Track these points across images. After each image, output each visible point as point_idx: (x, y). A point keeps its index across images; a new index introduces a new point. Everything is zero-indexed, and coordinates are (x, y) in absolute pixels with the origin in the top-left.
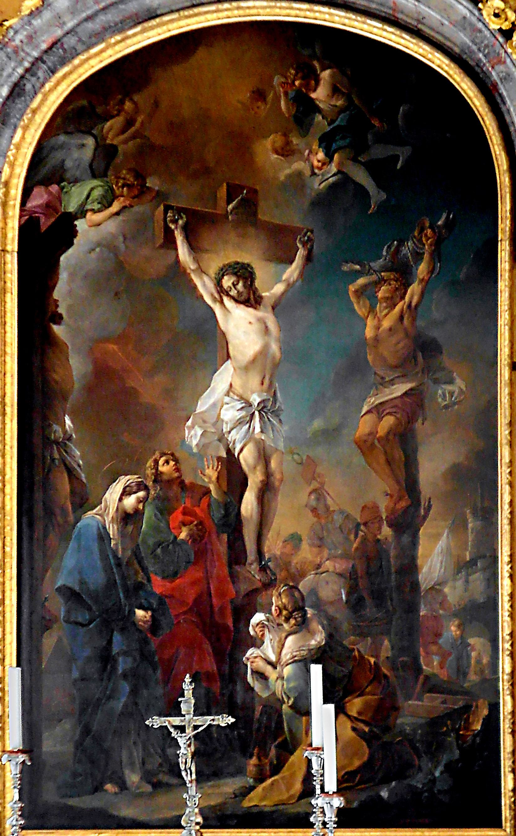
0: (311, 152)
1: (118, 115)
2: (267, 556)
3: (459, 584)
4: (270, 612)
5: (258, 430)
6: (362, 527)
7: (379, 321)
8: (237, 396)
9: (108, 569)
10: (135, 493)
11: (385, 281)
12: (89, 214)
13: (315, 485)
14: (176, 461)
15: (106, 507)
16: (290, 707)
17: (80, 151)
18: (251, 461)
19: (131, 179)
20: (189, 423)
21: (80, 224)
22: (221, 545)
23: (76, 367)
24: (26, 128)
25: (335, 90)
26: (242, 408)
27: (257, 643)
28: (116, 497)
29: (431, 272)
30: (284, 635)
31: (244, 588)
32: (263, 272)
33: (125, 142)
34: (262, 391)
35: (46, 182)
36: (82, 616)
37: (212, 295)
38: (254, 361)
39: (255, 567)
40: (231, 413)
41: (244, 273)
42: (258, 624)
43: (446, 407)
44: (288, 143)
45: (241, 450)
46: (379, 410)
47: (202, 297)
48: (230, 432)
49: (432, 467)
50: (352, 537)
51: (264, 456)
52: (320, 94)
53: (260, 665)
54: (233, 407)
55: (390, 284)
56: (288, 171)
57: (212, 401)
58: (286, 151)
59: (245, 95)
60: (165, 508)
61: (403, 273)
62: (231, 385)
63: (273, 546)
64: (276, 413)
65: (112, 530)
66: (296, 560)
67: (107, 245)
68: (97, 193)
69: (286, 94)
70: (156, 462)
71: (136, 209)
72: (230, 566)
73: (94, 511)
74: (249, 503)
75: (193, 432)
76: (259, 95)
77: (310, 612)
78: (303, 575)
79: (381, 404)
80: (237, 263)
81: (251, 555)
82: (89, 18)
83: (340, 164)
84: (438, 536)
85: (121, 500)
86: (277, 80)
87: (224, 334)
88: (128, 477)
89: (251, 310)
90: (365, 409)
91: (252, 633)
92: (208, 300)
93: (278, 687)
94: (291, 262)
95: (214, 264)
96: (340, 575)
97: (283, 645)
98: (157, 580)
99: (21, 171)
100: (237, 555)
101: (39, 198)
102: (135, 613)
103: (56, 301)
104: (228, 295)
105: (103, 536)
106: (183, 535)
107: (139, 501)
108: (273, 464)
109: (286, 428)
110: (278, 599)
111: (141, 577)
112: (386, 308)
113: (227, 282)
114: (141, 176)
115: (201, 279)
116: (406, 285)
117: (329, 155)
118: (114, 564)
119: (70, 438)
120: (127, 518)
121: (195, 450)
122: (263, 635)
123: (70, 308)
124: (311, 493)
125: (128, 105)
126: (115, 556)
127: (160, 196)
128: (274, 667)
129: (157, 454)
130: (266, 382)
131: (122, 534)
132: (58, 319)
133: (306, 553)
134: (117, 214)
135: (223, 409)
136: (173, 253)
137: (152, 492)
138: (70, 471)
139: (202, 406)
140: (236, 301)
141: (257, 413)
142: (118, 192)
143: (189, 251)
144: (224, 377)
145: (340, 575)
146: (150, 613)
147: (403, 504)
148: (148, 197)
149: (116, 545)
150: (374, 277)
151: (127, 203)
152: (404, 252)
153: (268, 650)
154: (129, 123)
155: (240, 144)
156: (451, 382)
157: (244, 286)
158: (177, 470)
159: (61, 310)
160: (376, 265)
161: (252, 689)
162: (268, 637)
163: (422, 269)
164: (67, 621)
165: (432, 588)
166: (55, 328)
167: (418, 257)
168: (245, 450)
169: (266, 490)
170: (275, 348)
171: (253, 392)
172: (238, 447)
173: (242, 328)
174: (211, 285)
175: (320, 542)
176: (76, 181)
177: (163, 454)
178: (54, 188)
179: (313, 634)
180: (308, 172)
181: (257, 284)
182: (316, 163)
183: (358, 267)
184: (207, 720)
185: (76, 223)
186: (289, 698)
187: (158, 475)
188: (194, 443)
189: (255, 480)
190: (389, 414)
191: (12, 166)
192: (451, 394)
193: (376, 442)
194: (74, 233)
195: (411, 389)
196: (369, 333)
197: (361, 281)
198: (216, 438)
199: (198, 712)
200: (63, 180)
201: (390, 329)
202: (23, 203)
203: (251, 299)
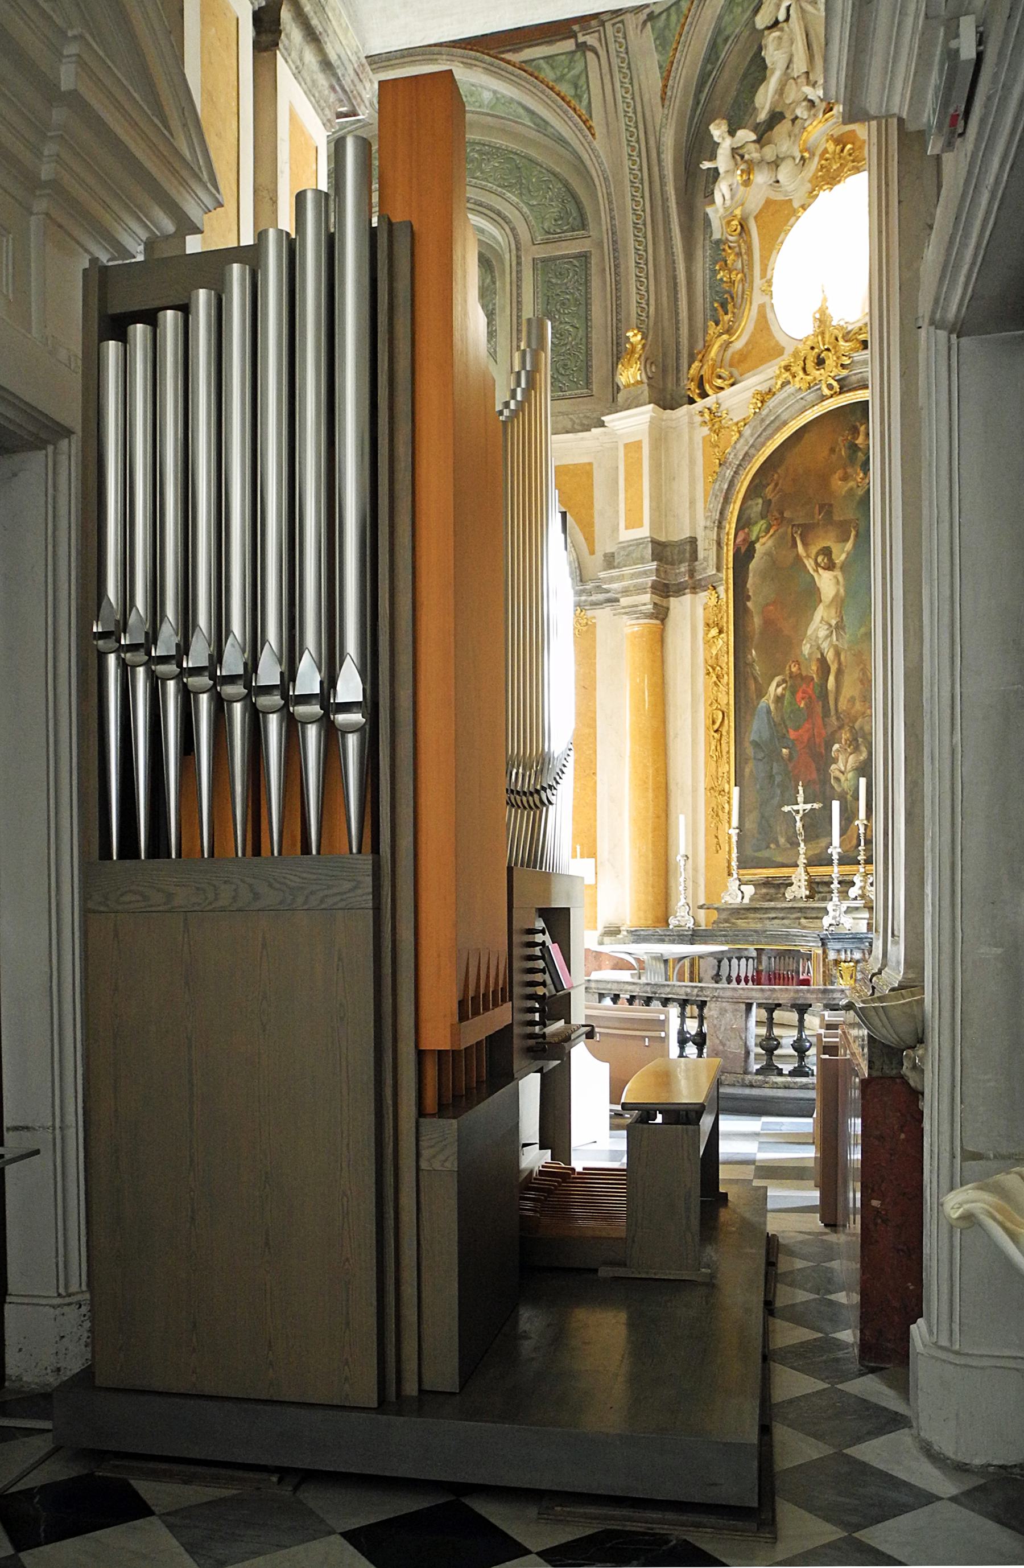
13: (862, 666)
18: (832, 658)
19: (778, 515)
21: (757, 546)
22: (819, 709)
23: (757, 621)
24: (735, 502)
27: (835, 761)
28: (774, 689)
31: (830, 730)
32: (835, 549)
35: (743, 528)
36: (761, 755)
38: (832, 601)
40: (822, 633)
41: (827, 552)
44: (846, 473)
51: (838, 654)
53: (837, 774)
58: (845, 478)
59: (826, 453)
63: (843, 705)
64: (843, 628)
65: (772, 707)
66: (853, 711)
67: (768, 554)
72: (823, 718)
76: (832, 450)
77: (860, 740)
78: (857, 720)
81: (833, 712)
82: (759, 436)
86: (840, 438)
87: (818, 589)
92: (811, 572)
93: (845, 785)
94: (847, 540)
95: (814, 550)
98: (791, 731)
99: (734, 525)
100: (826, 713)
105: (769, 711)
106: (802, 706)
107: (784, 689)
108: (842, 657)
110: (845, 735)
113: (820, 559)
114: (782, 513)
118: (773, 725)
120: (779, 699)
123: (754, 591)
125: (776, 476)
127: (790, 520)
128: (843, 773)
132: (748, 598)
138: (755, 678)
139: (809, 632)
140: (823, 568)
144: (820, 612)
148: (785, 522)
153: (841, 765)
154: (776, 485)
155: (824, 480)
158: (799, 669)
161: (833, 787)
170: (842, 591)
174: (813, 563)
176: (756, 523)
178: (746, 530)
181: (834, 557)
184: (808, 806)
187: (791, 672)
189: (834, 668)
191: (730, 523)
199: (805, 803)
203: (830, 567)
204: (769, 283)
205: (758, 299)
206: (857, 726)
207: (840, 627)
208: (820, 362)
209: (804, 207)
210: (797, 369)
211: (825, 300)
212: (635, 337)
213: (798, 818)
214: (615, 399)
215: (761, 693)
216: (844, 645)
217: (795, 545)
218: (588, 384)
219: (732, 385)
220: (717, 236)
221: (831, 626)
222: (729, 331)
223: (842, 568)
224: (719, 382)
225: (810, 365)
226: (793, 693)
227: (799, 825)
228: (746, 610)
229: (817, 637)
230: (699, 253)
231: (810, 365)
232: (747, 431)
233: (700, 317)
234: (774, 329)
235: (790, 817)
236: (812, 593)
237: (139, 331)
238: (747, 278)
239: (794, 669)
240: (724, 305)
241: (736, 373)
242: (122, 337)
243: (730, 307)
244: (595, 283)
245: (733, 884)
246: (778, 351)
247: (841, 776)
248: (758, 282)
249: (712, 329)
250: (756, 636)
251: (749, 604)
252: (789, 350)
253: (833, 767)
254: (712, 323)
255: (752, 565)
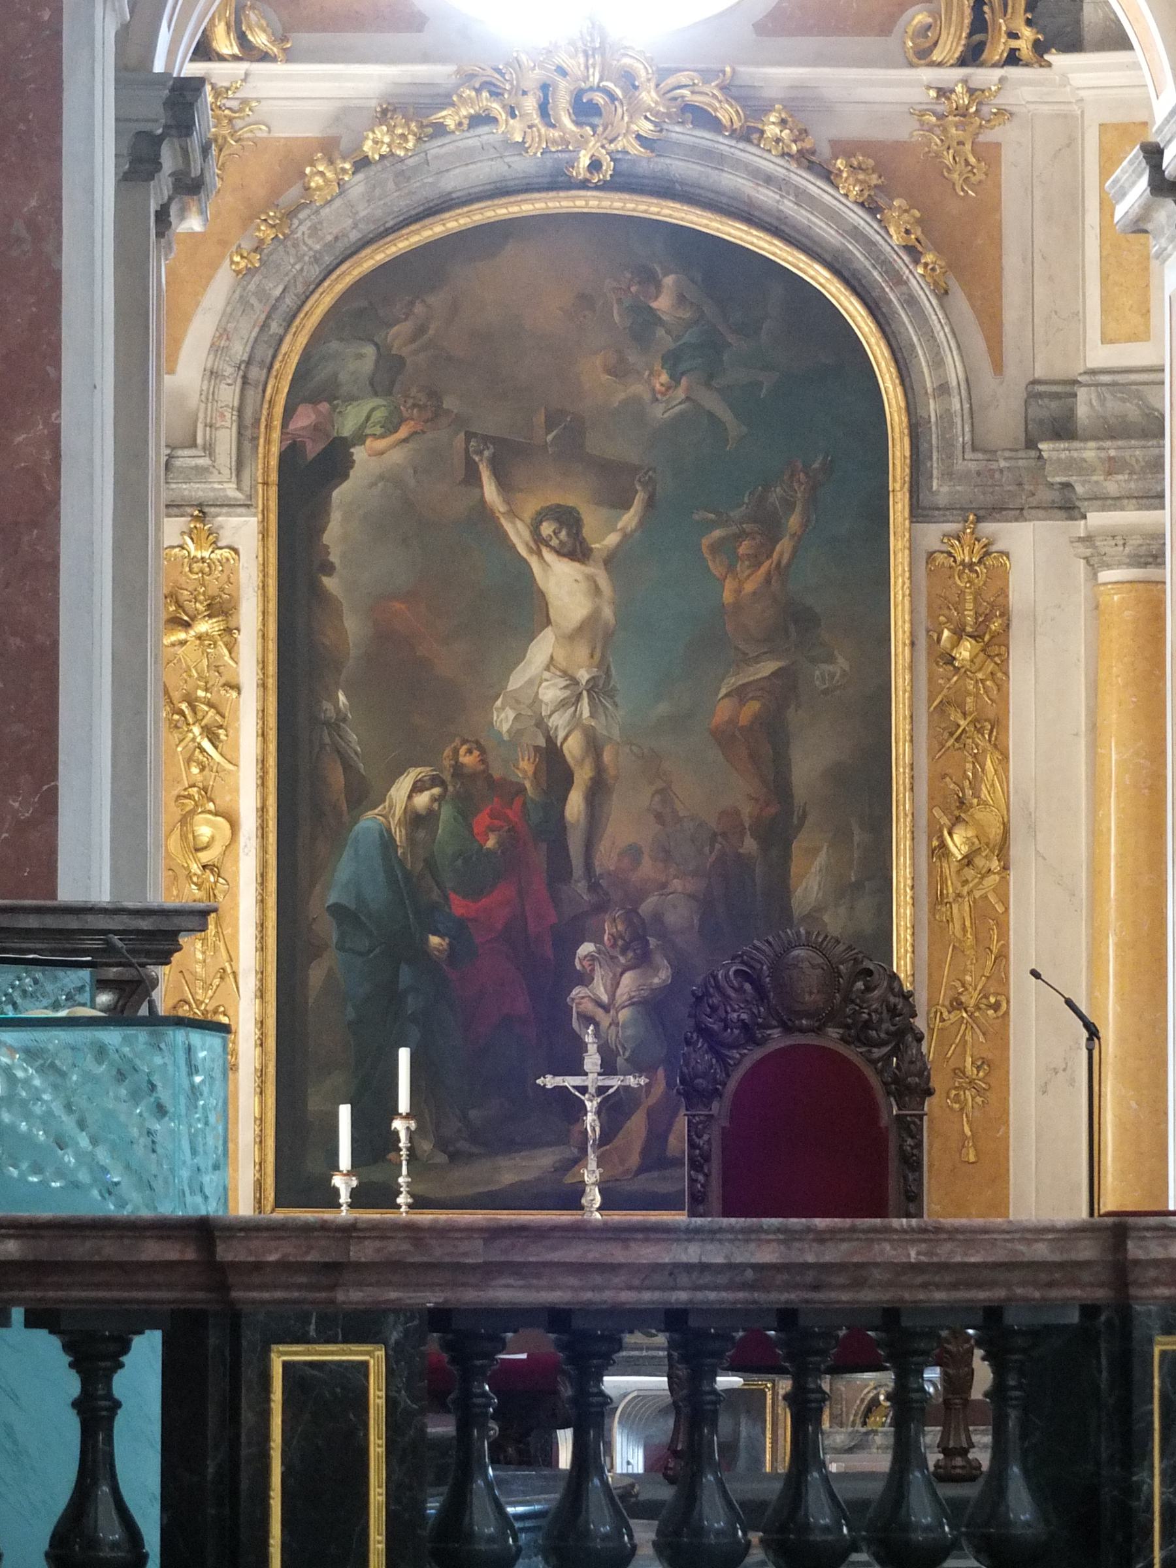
0: (651, 374)
1: (406, 319)
2: (598, 871)
3: (842, 910)
4: (601, 942)
5: (586, 713)
6: (719, 838)
7: (741, 583)
8: (561, 670)
9: (392, 881)
10: (428, 789)
11: (748, 535)
12: (368, 442)
13: (659, 784)
14: (483, 751)
15: (391, 807)
16: (626, 1060)
17: (359, 361)
19: (423, 399)
20: (499, 703)
22: (539, 857)
23: (353, 628)
25: (681, 299)
26: (566, 687)
27: (585, 979)
28: (403, 794)
29: (805, 525)
30: (619, 970)
32: (592, 519)
33: (416, 352)
34: (591, 666)
35: (313, 400)
37: (527, 545)
38: (580, 629)
39: (581, 887)
40: (551, 693)
41: (568, 519)
42: (586, 957)
43: (825, 692)
44: (622, 360)
45: (566, 739)
46: (740, 694)
47: (514, 547)
48: (550, 716)
49: (811, 761)
50: (707, 849)
51: (594, 745)
52: (663, 304)
53: (589, 1007)
54: (553, 685)
55: (754, 539)
56: (622, 396)
57: (527, 677)
60: (466, 805)
61: (769, 528)
62: (552, 657)
63: (607, 857)
64: (610, 694)
65: (399, 835)
67: (392, 479)
68: (378, 415)
69: (619, 301)
70: (456, 752)
71: (430, 435)
73: (376, 811)
74: (575, 805)
75: (503, 715)
77: (653, 942)
78: (642, 895)
79: (744, 685)
80: (559, 506)
83: (689, 389)
84: (815, 851)
85: (410, 797)
87: (542, 595)
88: (419, 769)
89: (576, 565)
90: (723, 691)
91: (578, 967)
92: (522, 550)
94: (627, 506)
95: (531, 506)
96: (691, 896)
97: (618, 983)
100: (559, 870)
101: (305, 418)
102: (427, 940)
103: (327, 547)
104: (548, 545)
105: (386, 841)
107: (434, 799)
108: (607, 757)
109: (622, 712)
111: (435, 895)
112: (749, 567)
113: (547, 529)
114: (434, 395)
115: (513, 523)
116: (775, 540)
117: (675, 379)
119: (344, 720)
120: (416, 821)
121: (506, 738)
122: (593, 970)
124: (653, 796)
125: (419, 309)
126: (403, 868)
128: (606, 1008)
129: (457, 741)
130: (598, 655)
131: (411, 840)
132: (328, 568)
133: (647, 868)
134: (405, 440)
135: (540, 685)
136: (478, 490)
137: (450, 788)
139: (516, 681)
140: (559, 553)
141: (585, 693)
142: (406, 414)
143: (498, 490)
144: (543, 648)
145: (691, 896)
146: (447, 940)
147: (772, 810)
149: (403, 853)
150: (734, 529)
151: (419, 428)
152: (771, 500)
154: (421, 330)
156: (830, 659)
157: (568, 534)
158: (483, 761)
159: (334, 558)
160: (735, 514)
162: (598, 974)
163: (794, 521)
164: (341, 947)
165: (808, 916)
166: (326, 581)
167: (790, 506)
168: (570, 740)
169: (598, 791)
170: (608, 613)
171: (580, 667)
172: (561, 735)
173: (565, 586)
174: (527, 535)
175: (665, 855)
176: (352, 399)
177: (464, 742)
178: (324, 407)
179: (656, 970)
180: (647, 397)
181: (586, 532)
182: (658, 386)
183: (712, 516)
185: (352, 450)
186: (624, 1048)
187: (458, 769)
188: (505, 728)
189: (583, 775)
190: (752, 698)
192: (832, 675)
193: (737, 733)
194: (349, 463)
195: (780, 669)
196: (728, 597)
197: (717, 533)
198: (533, 722)
200: (336, 398)
201: (754, 593)
202: (284, 425)
203: (577, 551)
206: (646, 907)
207: (599, 690)
215: (363, 795)
216: (610, 727)
217: (472, 477)
221: (574, 682)
223: (610, 561)
228: (318, 593)
229: (536, 700)
239: (468, 760)
247: (600, 1014)
250: (351, 663)
251: (330, 583)
253: (577, 992)
255: (341, 494)
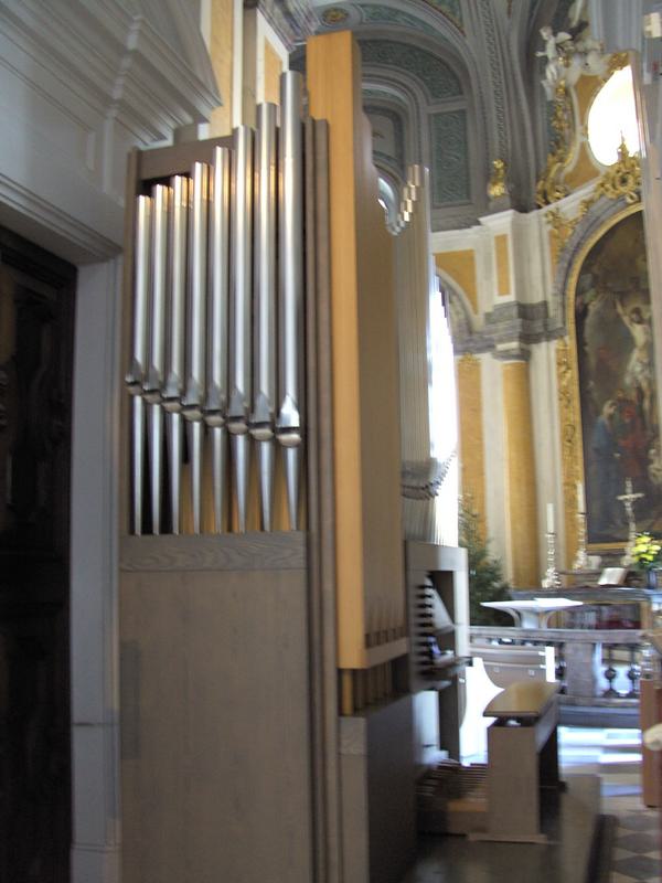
17: (588, 279)
27: (651, 462)
28: (608, 409)
40: (638, 369)
53: (653, 471)
67: (597, 313)
74: (646, 404)
100: (644, 428)
101: (579, 300)
120: (611, 417)
189: (648, 393)
199: (634, 492)
204: (586, 129)
205: (579, 138)
208: (624, 181)
209: (605, 80)
210: (608, 186)
211: (623, 139)
212: (498, 164)
213: (628, 504)
214: (489, 207)
215: (598, 412)
217: (615, 307)
218: (468, 196)
219: (566, 196)
220: (550, 98)
222: (562, 160)
224: (558, 194)
225: (617, 183)
226: (621, 412)
227: (629, 510)
230: (539, 110)
231: (617, 183)
232: (578, 227)
233: (541, 151)
234: (591, 158)
235: (621, 503)
236: (629, 341)
237: (159, 189)
238: (572, 126)
240: (557, 143)
241: (568, 187)
242: (149, 192)
243: (561, 144)
244: (470, 128)
245: (581, 554)
246: (595, 173)
248: (579, 128)
249: (551, 159)
252: (603, 173)
253: (652, 466)
254: (550, 155)
